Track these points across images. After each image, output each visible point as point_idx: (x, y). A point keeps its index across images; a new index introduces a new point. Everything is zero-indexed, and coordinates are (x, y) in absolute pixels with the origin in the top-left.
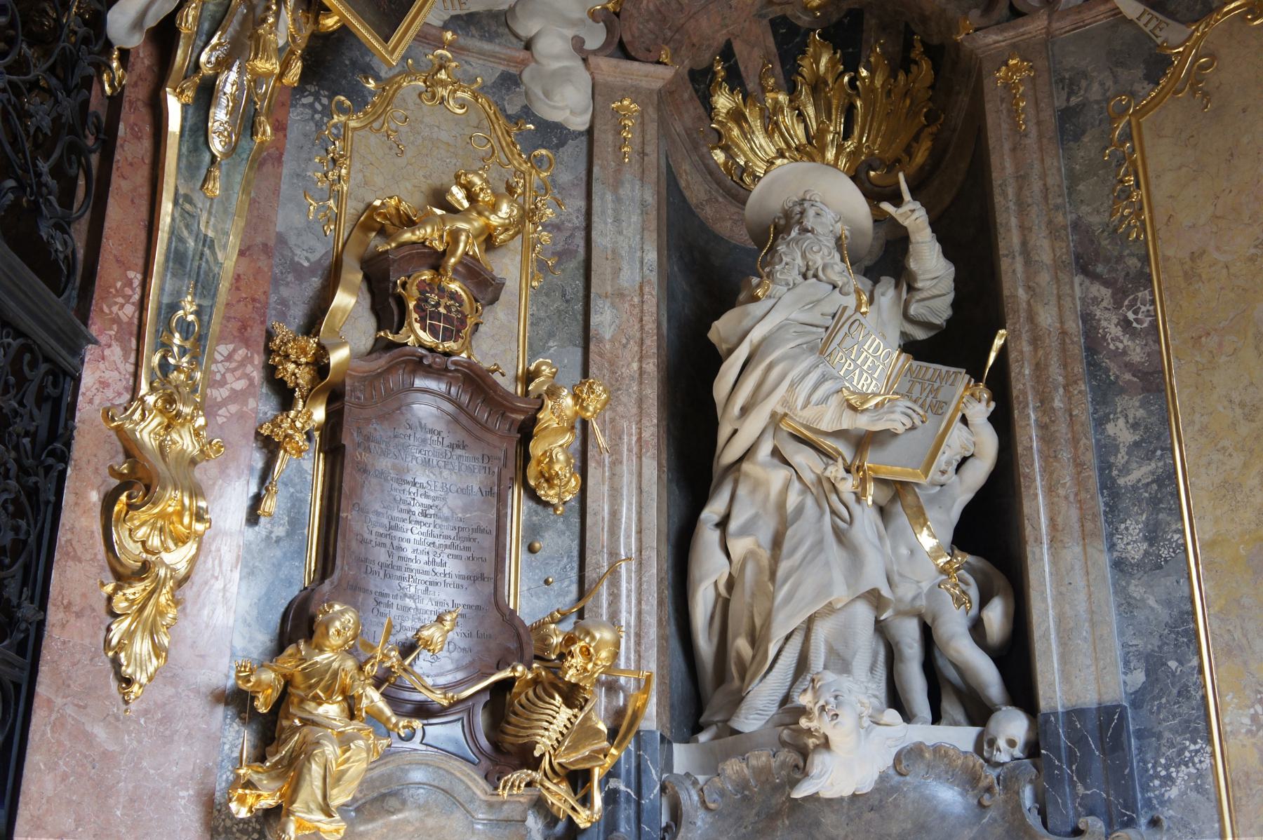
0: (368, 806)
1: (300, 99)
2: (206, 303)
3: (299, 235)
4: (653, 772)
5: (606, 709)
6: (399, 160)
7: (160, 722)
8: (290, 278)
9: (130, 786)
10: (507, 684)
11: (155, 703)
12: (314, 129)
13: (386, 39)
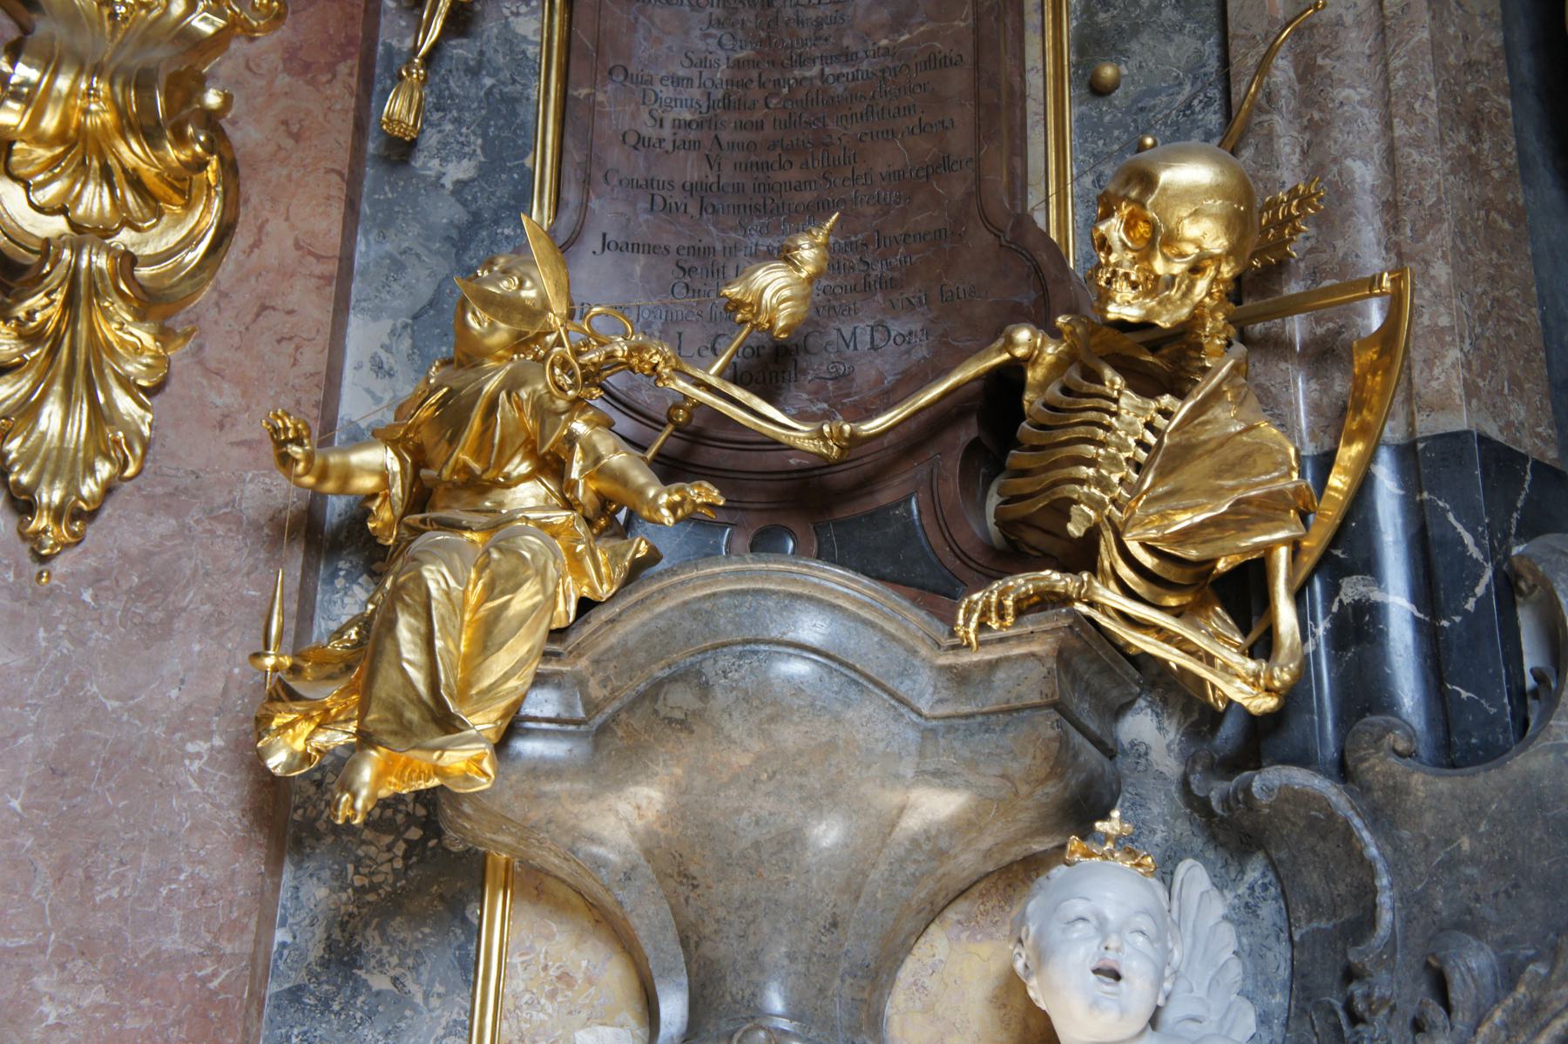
0: (623, 716)
4: (1468, 539)
5: (1315, 409)
7: (138, 593)
9: (51, 742)
10: (1009, 379)
11: (124, 554)
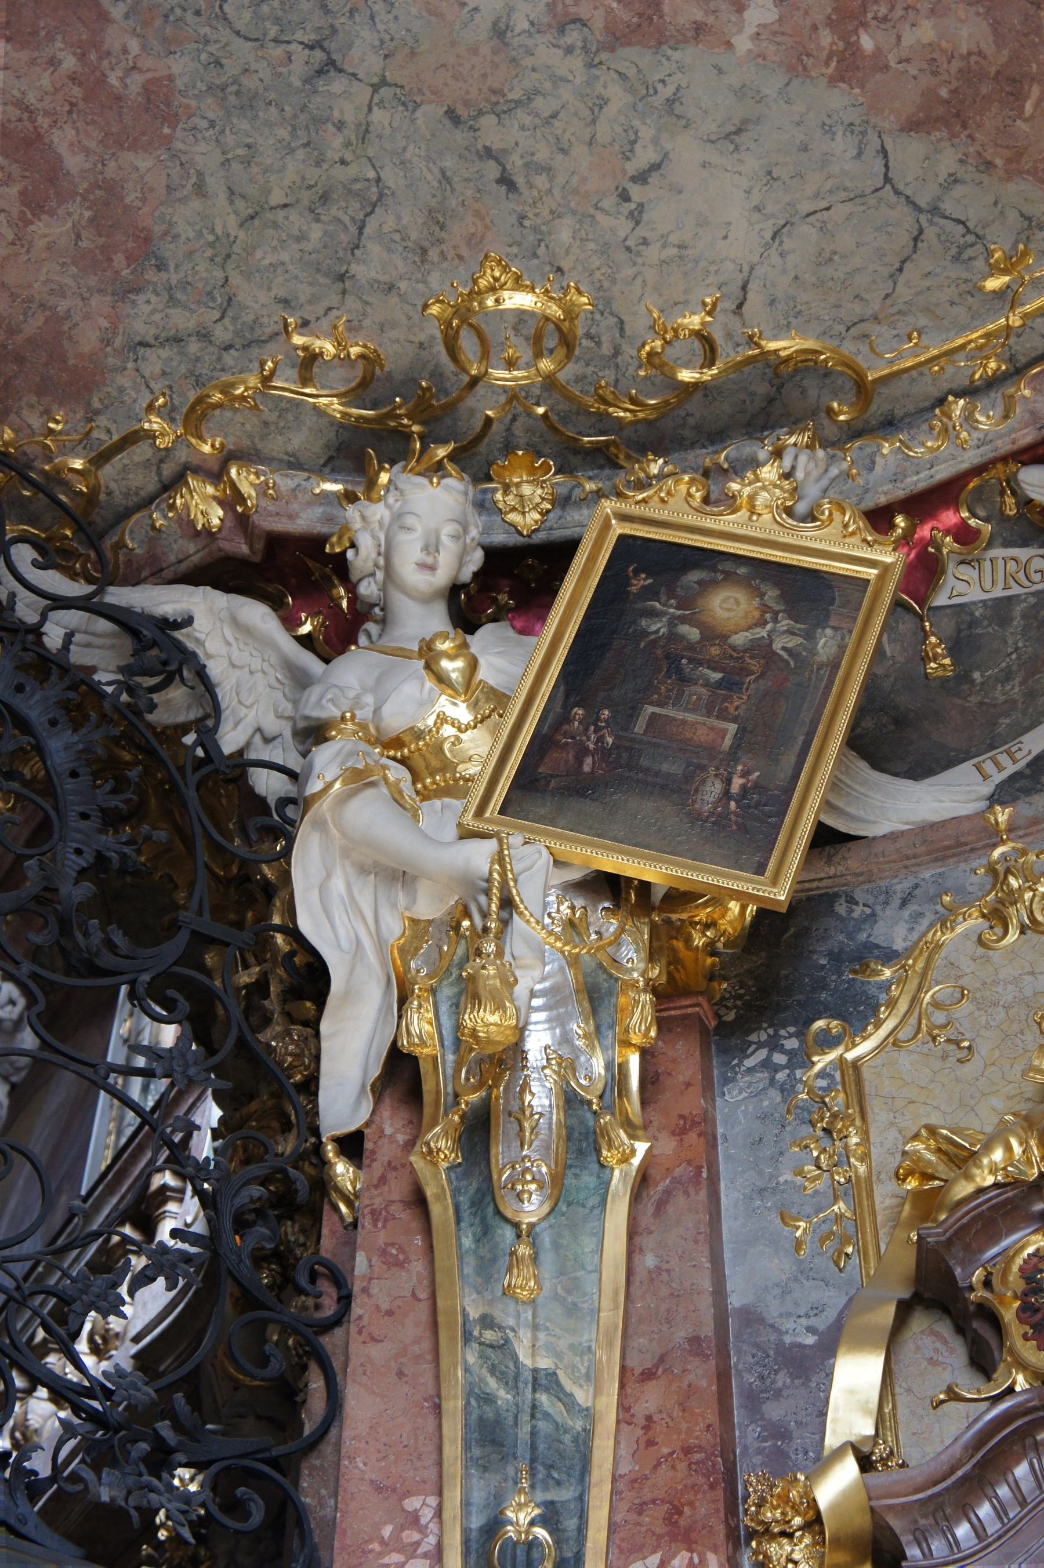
1: (741, 1062)
2: (566, 1494)
3: (786, 1292)
6: (967, 1068)
8: (782, 1379)
12: (779, 1099)
13: (760, 870)
